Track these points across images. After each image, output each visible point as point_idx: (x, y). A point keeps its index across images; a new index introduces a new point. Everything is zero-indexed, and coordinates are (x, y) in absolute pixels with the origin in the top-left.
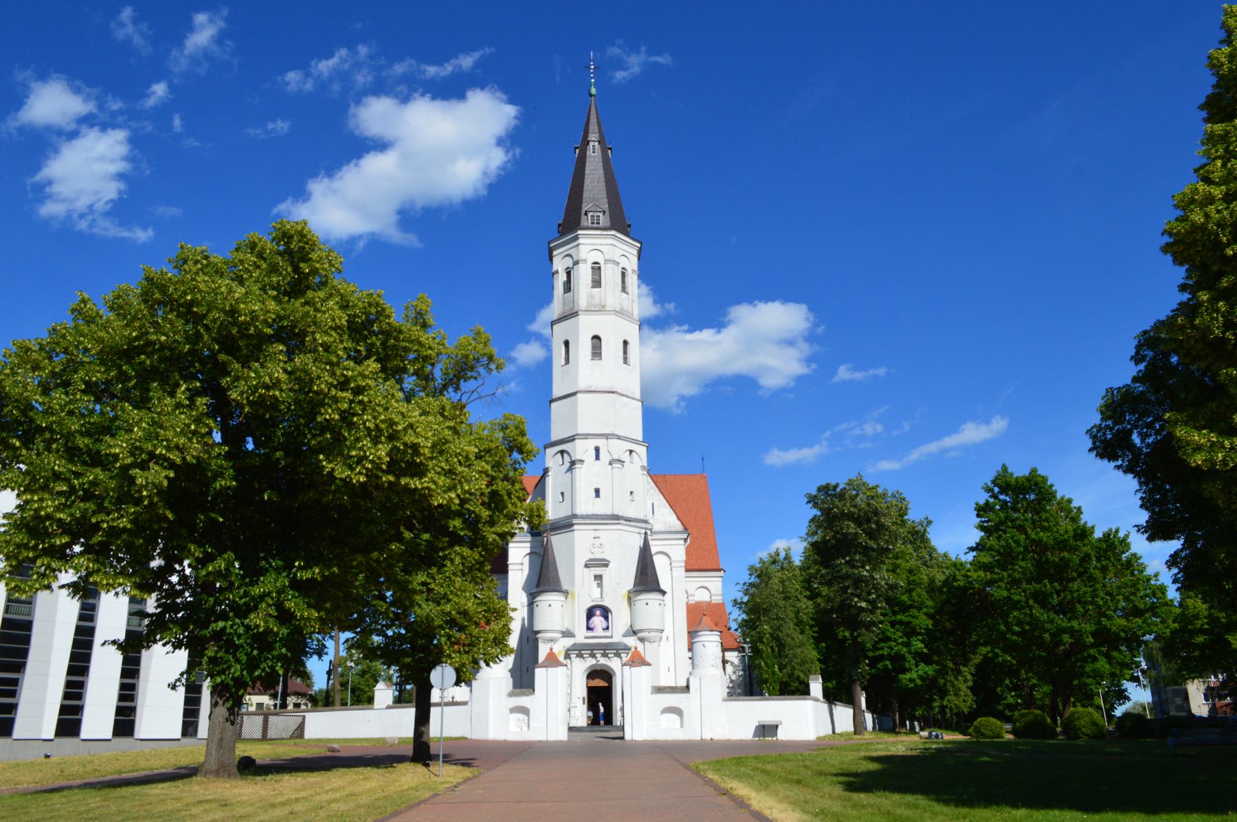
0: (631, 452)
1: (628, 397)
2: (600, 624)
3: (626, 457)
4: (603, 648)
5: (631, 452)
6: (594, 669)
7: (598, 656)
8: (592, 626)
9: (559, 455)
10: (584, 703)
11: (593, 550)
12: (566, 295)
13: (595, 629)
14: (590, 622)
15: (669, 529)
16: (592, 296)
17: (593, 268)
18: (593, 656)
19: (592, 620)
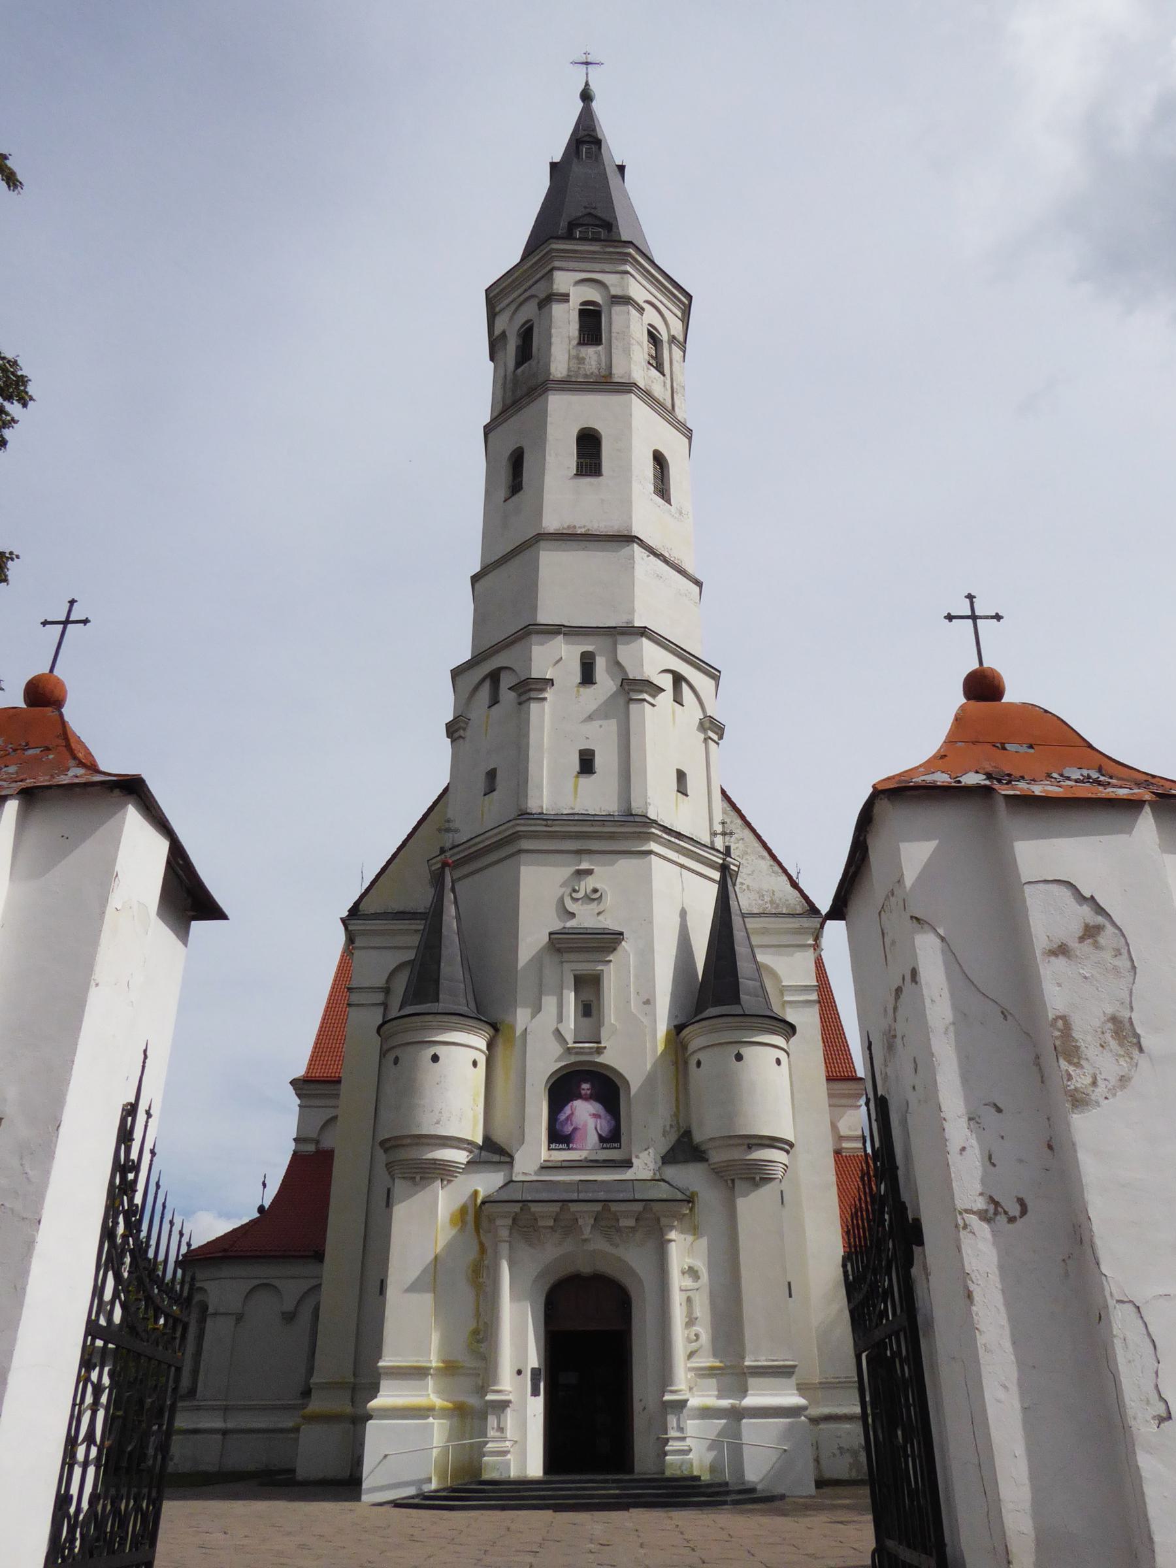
0: (678, 679)
1: (666, 561)
2: (591, 1123)
3: (666, 682)
4: (602, 1195)
5: (678, 679)
6: (563, 1273)
7: (586, 1224)
8: (568, 1129)
9: (487, 686)
10: (535, 1393)
11: (571, 906)
12: (520, 370)
13: (578, 1135)
14: (562, 1117)
15: (770, 908)
16: (581, 360)
17: (581, 312)
18: (566, 1225)
19: (567, 1110)
